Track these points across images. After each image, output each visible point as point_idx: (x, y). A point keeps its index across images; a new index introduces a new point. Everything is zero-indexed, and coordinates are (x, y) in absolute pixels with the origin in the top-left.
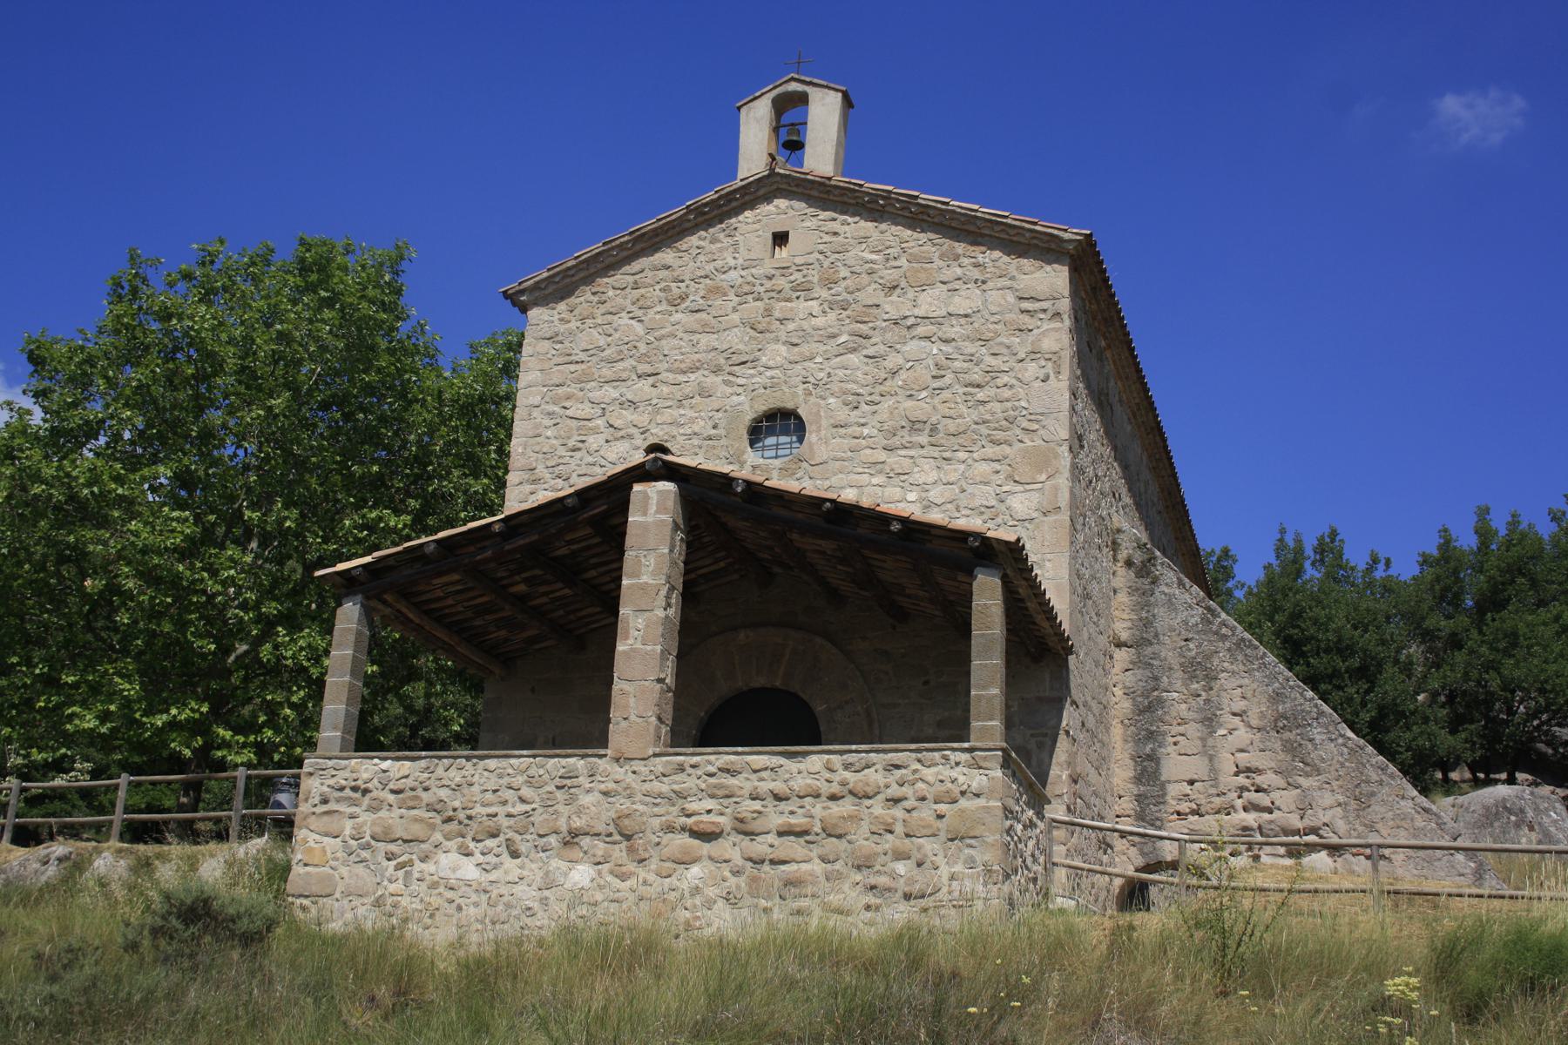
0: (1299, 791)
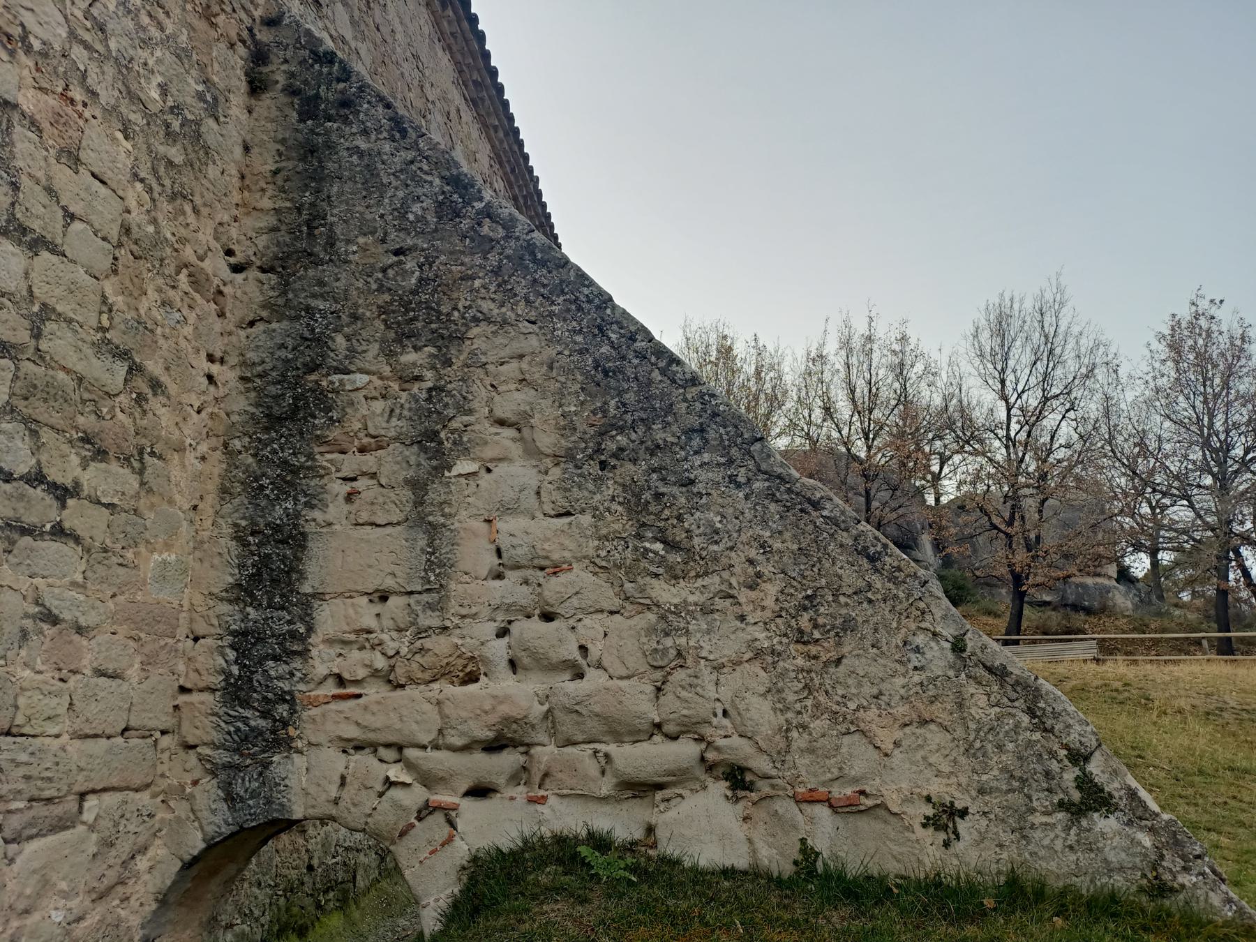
0: (652, 617)
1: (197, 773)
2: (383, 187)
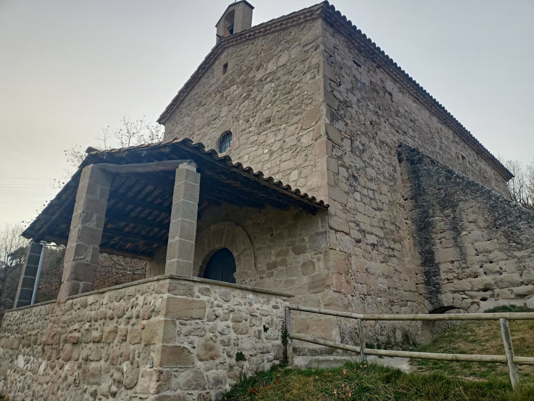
0: (516, 260)
1: (424, 299)
2: (432, 176)
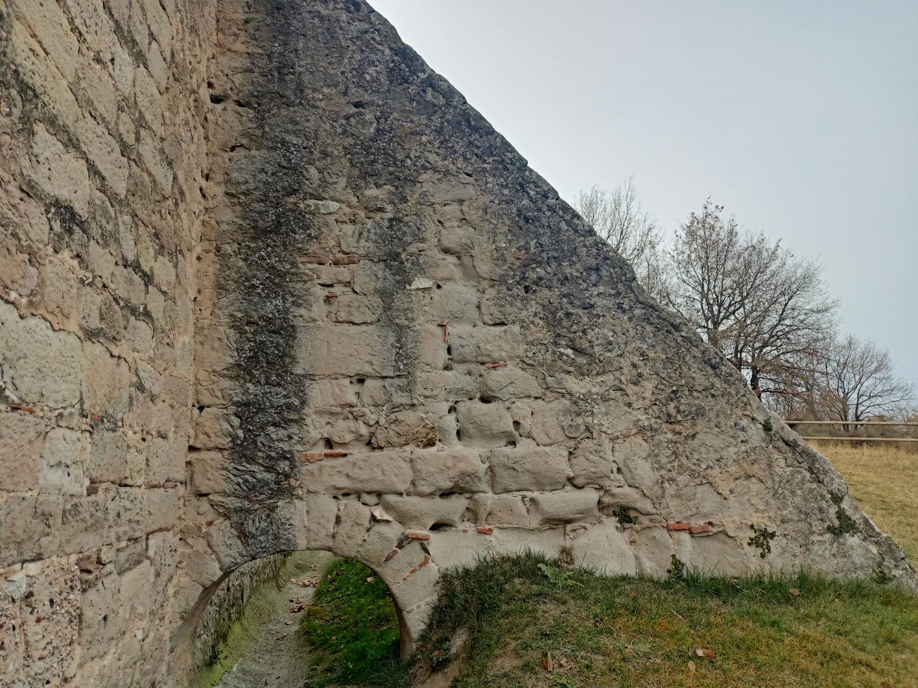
1: (211, 516)
2: (343, 50)
